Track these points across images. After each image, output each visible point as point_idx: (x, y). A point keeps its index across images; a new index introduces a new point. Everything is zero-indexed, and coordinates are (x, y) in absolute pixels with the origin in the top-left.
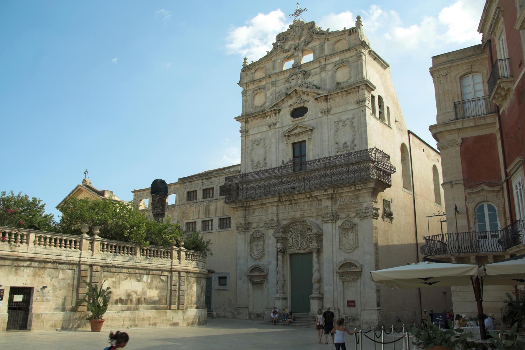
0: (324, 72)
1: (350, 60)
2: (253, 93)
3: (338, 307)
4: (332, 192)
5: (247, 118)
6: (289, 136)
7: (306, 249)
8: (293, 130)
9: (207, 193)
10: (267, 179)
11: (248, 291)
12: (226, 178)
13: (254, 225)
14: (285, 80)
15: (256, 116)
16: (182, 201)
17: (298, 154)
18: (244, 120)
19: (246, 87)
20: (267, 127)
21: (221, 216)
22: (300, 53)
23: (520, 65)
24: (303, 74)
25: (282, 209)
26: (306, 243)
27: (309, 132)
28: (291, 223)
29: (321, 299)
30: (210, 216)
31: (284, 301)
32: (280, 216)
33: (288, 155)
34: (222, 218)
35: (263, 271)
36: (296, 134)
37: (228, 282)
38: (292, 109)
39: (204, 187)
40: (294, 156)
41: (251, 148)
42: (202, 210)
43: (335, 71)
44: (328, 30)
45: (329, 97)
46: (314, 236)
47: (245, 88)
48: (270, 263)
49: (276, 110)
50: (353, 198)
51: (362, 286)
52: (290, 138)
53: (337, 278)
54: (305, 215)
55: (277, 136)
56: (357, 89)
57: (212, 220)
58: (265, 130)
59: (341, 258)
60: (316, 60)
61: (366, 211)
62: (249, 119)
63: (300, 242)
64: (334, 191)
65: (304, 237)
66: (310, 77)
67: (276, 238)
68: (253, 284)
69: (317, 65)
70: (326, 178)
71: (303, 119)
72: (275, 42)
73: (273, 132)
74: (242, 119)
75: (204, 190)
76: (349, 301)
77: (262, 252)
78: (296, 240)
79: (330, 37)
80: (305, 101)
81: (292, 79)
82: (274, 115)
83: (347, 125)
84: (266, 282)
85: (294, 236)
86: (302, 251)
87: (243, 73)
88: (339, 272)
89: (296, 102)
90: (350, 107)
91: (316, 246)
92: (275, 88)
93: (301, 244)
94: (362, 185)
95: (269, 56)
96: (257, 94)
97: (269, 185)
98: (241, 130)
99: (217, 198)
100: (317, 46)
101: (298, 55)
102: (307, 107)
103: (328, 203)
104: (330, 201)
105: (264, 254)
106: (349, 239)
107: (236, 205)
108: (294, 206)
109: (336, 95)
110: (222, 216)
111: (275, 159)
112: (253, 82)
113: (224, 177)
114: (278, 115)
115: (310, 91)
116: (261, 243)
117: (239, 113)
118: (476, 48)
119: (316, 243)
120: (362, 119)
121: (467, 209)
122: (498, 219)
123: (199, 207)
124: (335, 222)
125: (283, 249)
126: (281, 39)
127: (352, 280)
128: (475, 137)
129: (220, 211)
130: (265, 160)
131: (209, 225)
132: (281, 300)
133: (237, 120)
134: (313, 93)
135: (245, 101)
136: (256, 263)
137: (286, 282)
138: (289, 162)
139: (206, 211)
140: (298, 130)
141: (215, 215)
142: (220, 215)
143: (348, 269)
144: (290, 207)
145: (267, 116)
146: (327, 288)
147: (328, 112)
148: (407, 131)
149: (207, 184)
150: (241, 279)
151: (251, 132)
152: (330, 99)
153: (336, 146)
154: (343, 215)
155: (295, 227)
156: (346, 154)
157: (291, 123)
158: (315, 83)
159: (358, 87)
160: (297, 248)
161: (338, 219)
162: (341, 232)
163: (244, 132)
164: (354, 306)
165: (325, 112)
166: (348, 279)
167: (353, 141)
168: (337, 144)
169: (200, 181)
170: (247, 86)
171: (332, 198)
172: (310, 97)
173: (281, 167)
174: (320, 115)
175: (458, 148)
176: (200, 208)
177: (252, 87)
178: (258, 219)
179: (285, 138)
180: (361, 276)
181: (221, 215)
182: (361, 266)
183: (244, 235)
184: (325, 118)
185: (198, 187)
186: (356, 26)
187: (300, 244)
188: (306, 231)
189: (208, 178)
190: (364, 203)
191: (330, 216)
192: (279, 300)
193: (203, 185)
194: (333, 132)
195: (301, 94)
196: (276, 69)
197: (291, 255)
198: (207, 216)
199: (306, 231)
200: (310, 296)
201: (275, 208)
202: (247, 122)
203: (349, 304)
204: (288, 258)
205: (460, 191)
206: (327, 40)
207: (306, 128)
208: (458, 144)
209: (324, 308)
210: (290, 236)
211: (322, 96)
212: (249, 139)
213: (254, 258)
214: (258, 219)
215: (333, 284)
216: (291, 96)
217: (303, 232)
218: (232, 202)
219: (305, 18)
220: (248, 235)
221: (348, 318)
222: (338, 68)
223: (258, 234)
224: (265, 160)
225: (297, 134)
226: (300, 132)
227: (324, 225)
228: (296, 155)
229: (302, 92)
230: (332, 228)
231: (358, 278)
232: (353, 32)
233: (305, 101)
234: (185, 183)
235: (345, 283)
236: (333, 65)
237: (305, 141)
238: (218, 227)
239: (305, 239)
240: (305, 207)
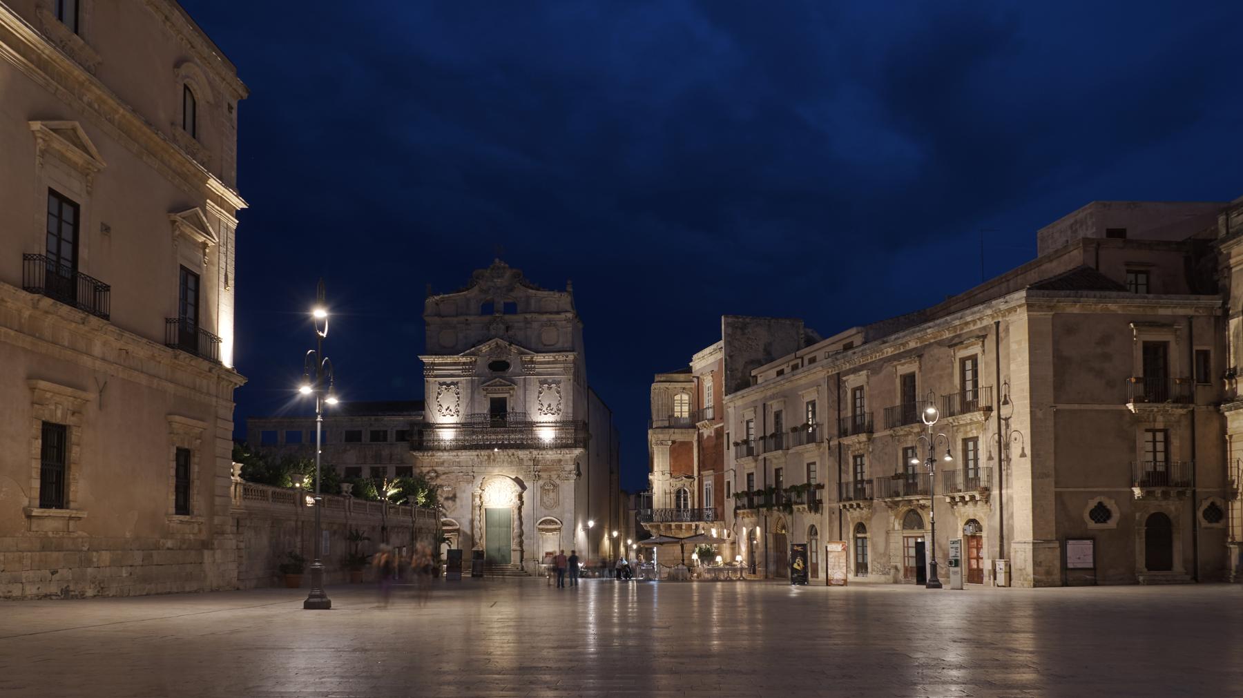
39: (373, 429)
75: (372, 432)
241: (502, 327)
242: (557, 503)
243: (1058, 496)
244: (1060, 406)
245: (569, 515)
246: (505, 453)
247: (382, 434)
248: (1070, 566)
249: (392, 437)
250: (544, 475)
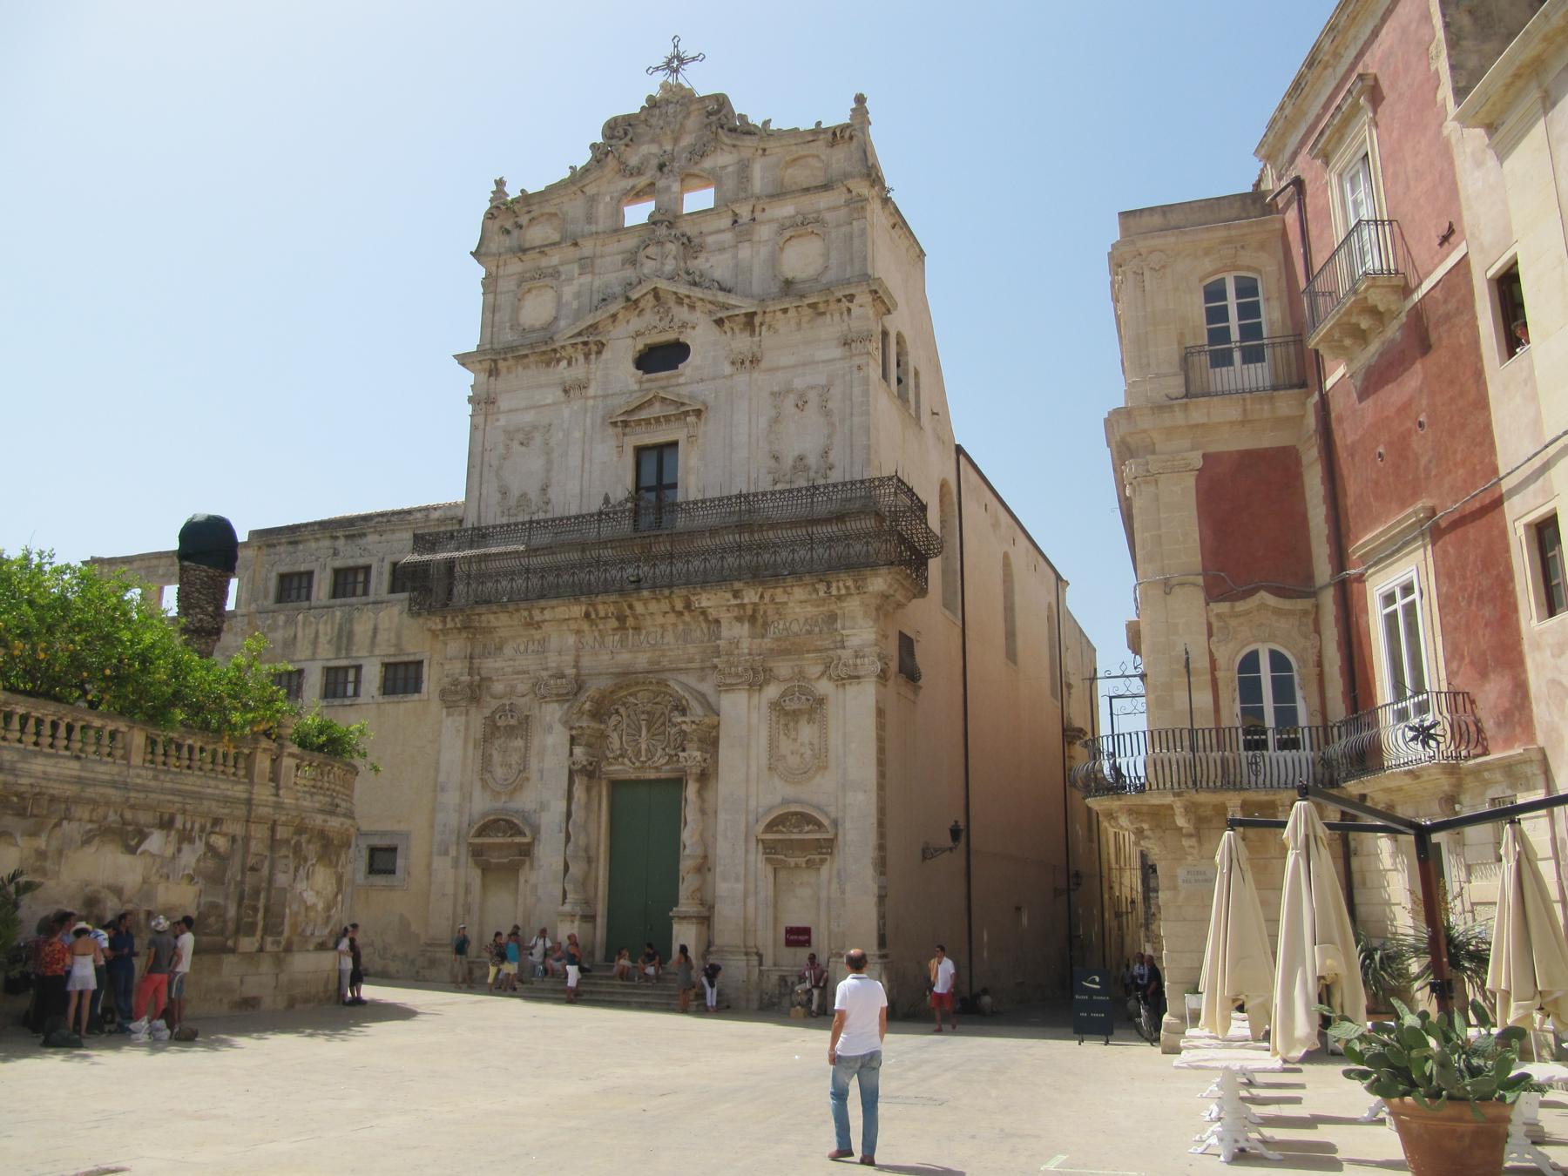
0: (747, 244)
1: (828, 216)
2: (519, 286)
3: (756, 946)
4: (756, 599)
5: (495, 361)
6: (626, 424)
7: (664, 768)
8: (639, 407)
9: (348, 582)
10: (549, 549)
11: (467, 891)
12: (415, 536)
13: (498, 687)
14: (625, 255)
15: (526, 356)
16: (259, 602)
17: (649, 479)
18: (486, 365)
19: (498, 267)
20: (559, 393)
21: (390, 655)
22: (676, 181)
23: (1445, 239)
24: (683, 244)
25: (591, 642)
26: (664, 749)
27: (691, 419)
29: (705, 920)
30: (354, 655)
31: (584, 925)
33: (620, 482)
34: (392, 660)
36: (648, 421)
37: (400, 862)
38: (640, 346)
39: (339, 563)
40: (638, 487)
42: (326, 634)
43: (781, 245)
44: (767, 123)
45: (757, 320)
46: (694, 726)
47: (494, 269)
48: (543, 806)
49: (591, 344)
50: (817, 621)
51: (834, 886)
52: (627, 430)
53: (758, 860)
54: (665, 662)
55: (588, 421)
56: (844, 303)
57: (358, 668)
58: (549, 401)
59: (772, 795)
60: (722, 203)
61: (858, 661)
62: (501, 364)
63: (644, 747)
64: (762, 597)
65: (660, 730)
66: (702, 257)
67: (572, 728)
68: (483, 870)
70: (740, 556)
71: (674, 376)
72: (599, 140)
73: (576, 408)
74: (480, 361)
75: (337, 572)
76: (791, 928)
77: (520, 771)
78: (632, 738)
79: (771, 145)
80: (683, 326)
81: (647, 257)
82: (581, 358)
83: (809, 403)
84: (528, 864)
85: (628, 725)
86: (652, 775)
87: (490, 222)
88: (762, 840)
89: (655, 327)
90: (821, 355)
91: (699, 758)
92: (587, 278)
93: (648, 750)
94: (850, 583)
95: (578, 178)
96: (529, 290)
97: (559, 568)
98: (471, 394)
99: (379, 599)
100: (730, 169)
101: (668, 188)
102: (688, 342)
103: (743, 630)
104: (746, 626)
105: (528, 779)
106: (799, 741)
107: (444, 622)
108: (630, 638)
109: (779, 314)
110: (394, 655)
111: (577, 490)
112: (520, 254)
113: (408, 535)
114: (596, 359)
115: (700, 295)
116: (519, 743)
117: (471, 343)
118: (1249, 202)
119: (699, 749)
120: (857, 390)
121: (1213, 661)
122: (1299, 694)
123: (317, 624)
124: (760, 690)
125: (591, 764)
126: (617, 134)
127: (804, 865)
128: (1238, 451)
129: (389, 640)
130: (544, 490)
131: (346, 682)
132: (577, 923)
133: (463, 365)
134: (710, 302)
135: (490, 309)
137: (594, 865)
138: (627, 500)
139: (340, 637)
140: (657, 410)
141: (371, 651)
142: (385, 650)
143: (795, 830)
144: (617, 637)
145: (558, 361)
146: (726, 889)
147: (751, 362)
148: (953, 448)
149: (350, 556)
150: (446, 853)
151: (504, 403)
152: (761, 324)
153: (772, 463)
154: (783, 668)
155: (632, 700)
156: (808, 489)
157: (636, 387)
158: (718, 274)
159: (851, 298)
160: (634, 764)
161: (767, 682)
162: (774, 719)
163: (482, 402)
164: (807, 943)
165: (742, 363)
166: (792, 861)
168: (776, 458)
169: (327, 543)
170: (501, 263)
171: (753, 619)
172: (698, 314)
173: (600, 513)
174: (727, 369)
175: (1190, 481)
176: (321, 627)
178: (510, 669)
179: (611, 431)
180: (831, 854)
181: (392, 650)
182: (835, 823)
183: (464, 718)
184: (742, 379)
185: (321, 563)
187: (643, 753)
188: (667, 712)
189: (354, 536)
190: (852, 638)
191: (746, 670)
192: (573, 922)
193: (336, 553)
194: (763, 422)
195: (672, 303)
196: (596, 223)
197: (616, 785)
198: (344, 652)
199: (667, 712)
200: (671, 910)
201: (571, 640)
202: (493, 372)
203: (792, 937)
204: (604, 793)
205: (1190, 607)
206: (760, 152)
207: (683, 404)
208: (1191, 470)
209: (712, 949)
210: (616, 725)
211: (737, 315)
212: (498, 424)
213: (493, 791)
214: (510, 669)
215: (746, 876)
216: (642, 304)
217: (657, 715)
218: (431, 611)
219: (700, 81)
220: (477, 719)
221: (786, 982)
222: (791, 237)
223: (512, 717)
224: (544, 490)
225: (652, 421)
226: (664, 416)
227: (723, 695)
228: (644, 483)
229: (674, 297)
230: (749, 707)
231: (823, 861)
232: (842, 137)
233: (684, 325)
234: (274, 546)
235: (782, 874)
236: (775, 226)
237: (675, 444)
238: (379, 689)
239: (661, 738)
240: (665, 641)
242: (820, 760)
245: (860, 796)
246: (665, 605)
249: (380, 582)
250: (783, 668)
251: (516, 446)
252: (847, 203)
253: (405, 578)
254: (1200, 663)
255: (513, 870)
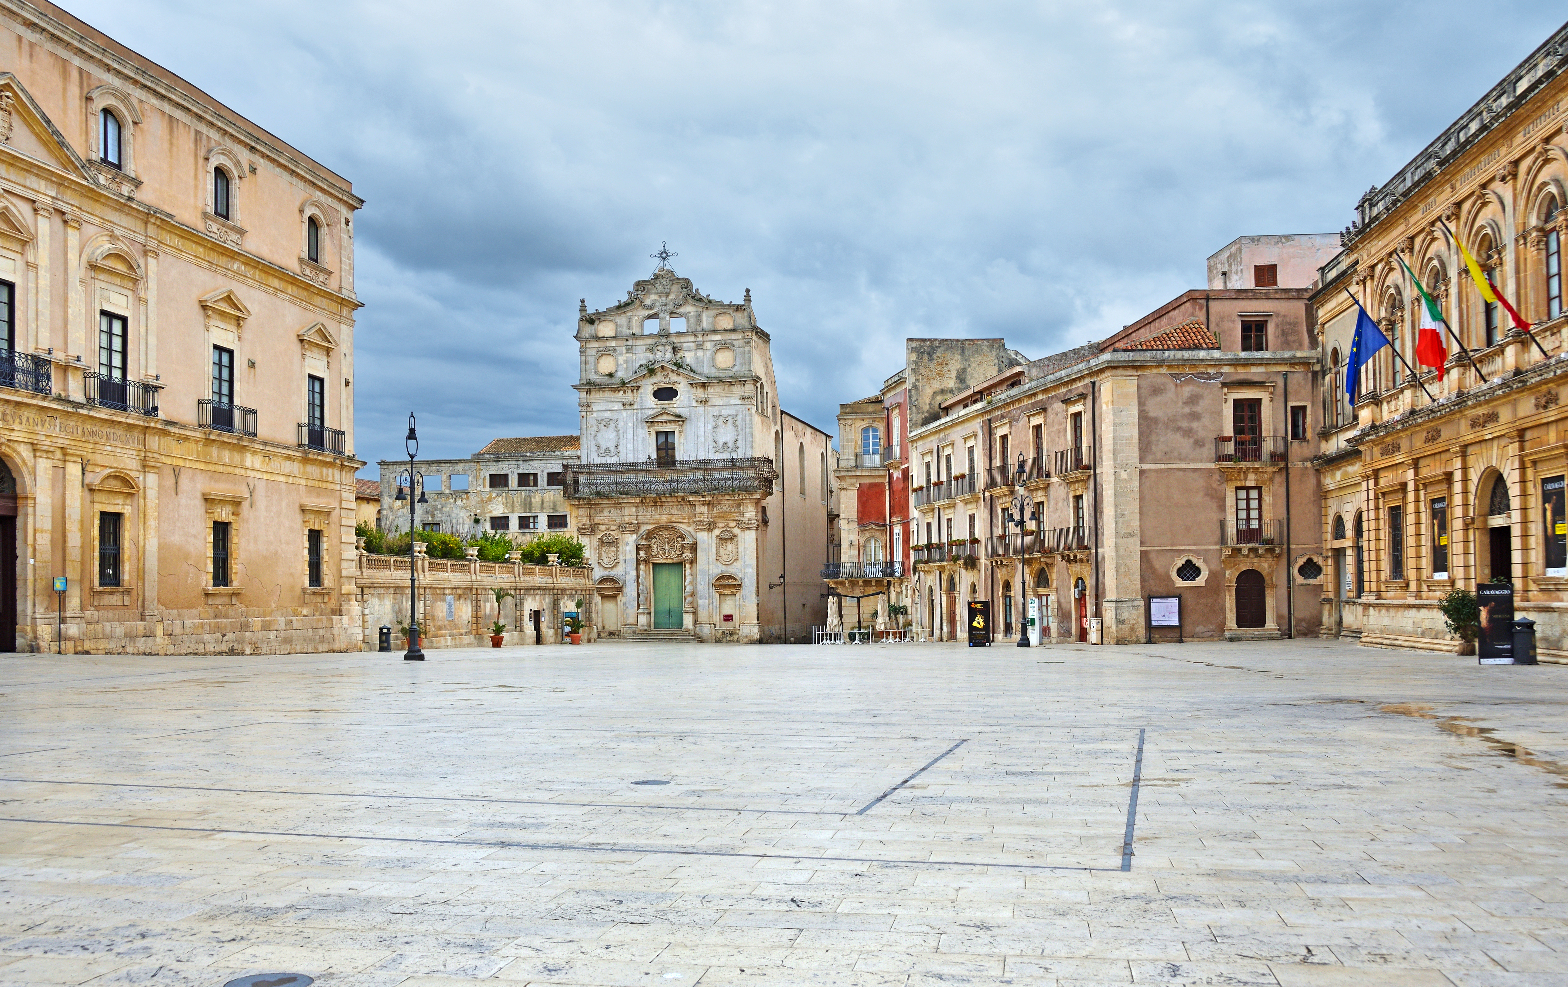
1: (735, 343)
13: (603, 527)
28: (656, 528)
32: (640, 518)
35: (616, 582)
41: (595, 428)
57: (535, 517)
69: (691, 339)
103: (704, 509)
120: (748, 419)
130: (617, 447)
136: (606, 573)
140: (665, 418)
149: (525, 469)
151: (595, 407)
167: (735, 442)
174: (695, 404)
177: (595, 344)
184: (701, 409)
186: (743, 303)
194: (710, 427)
224: (617, 447)
241: (670, 348)
243: (1144, 555)
244: (1145, 466)
247: (531, 478)
248: (1154, 623)
249: (542, 480)
251: (602, 426)
252: (743, 338)
253: (553, 479)
254: (855, 543)
255: (614, 597)
